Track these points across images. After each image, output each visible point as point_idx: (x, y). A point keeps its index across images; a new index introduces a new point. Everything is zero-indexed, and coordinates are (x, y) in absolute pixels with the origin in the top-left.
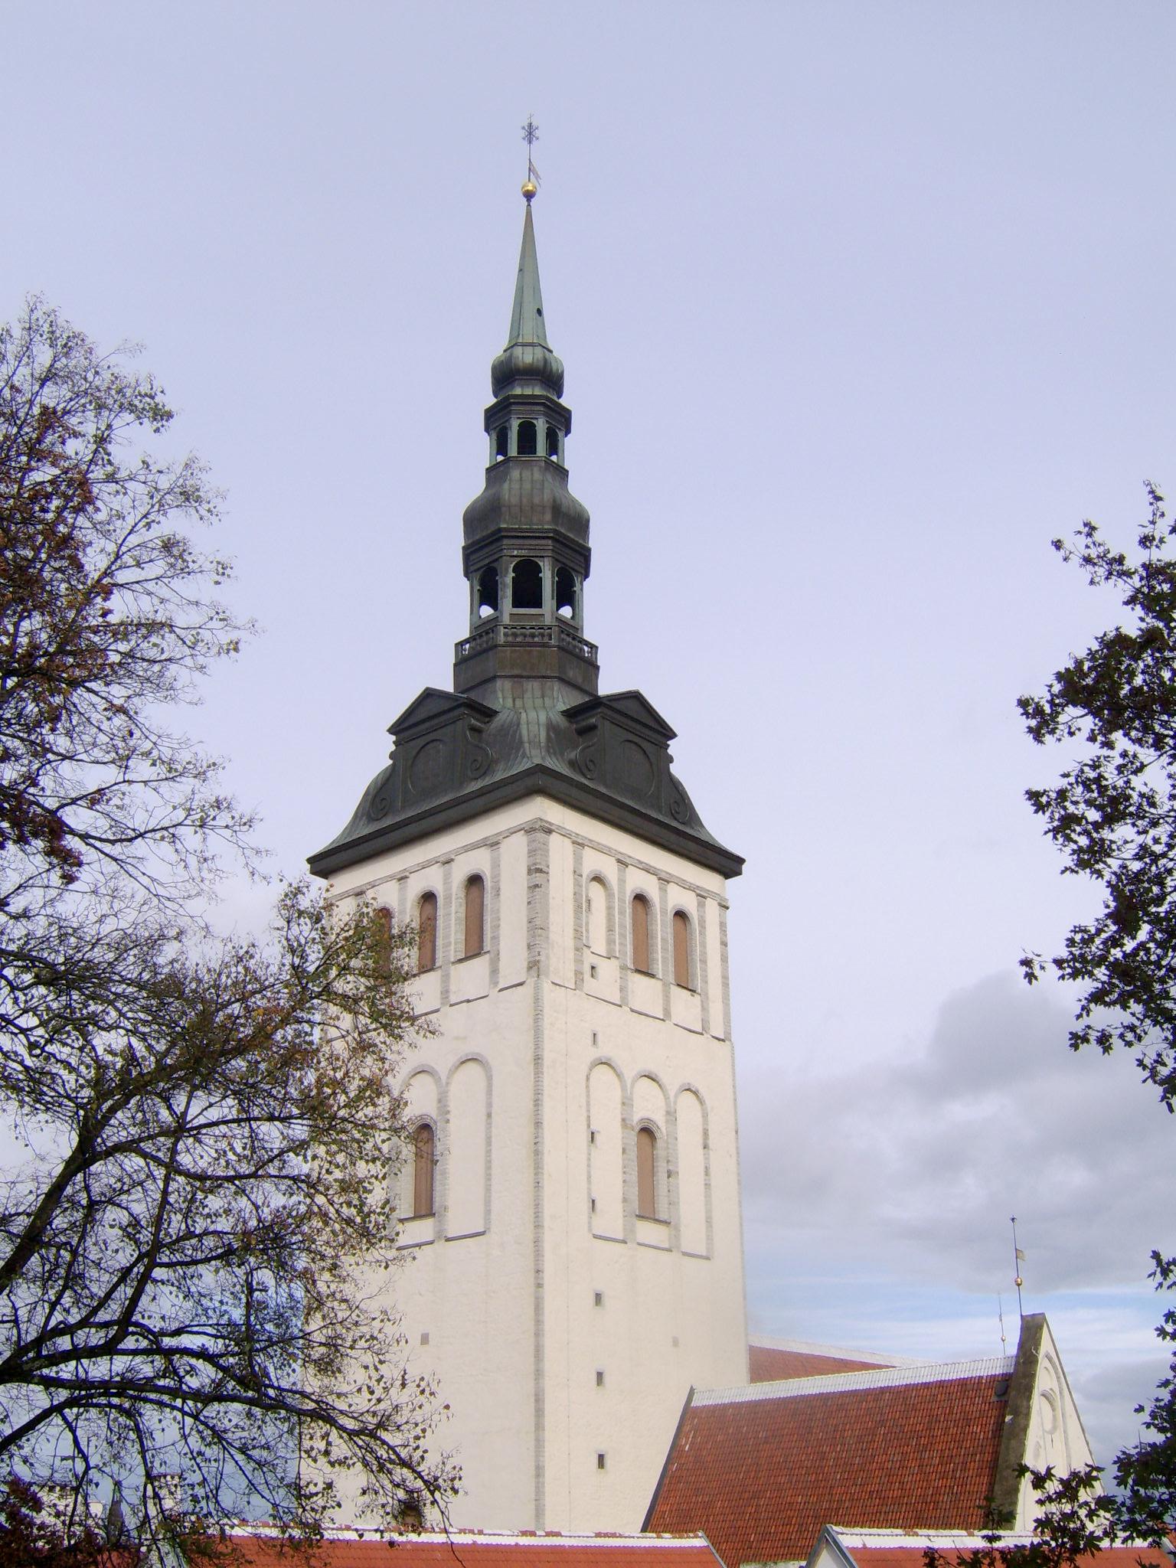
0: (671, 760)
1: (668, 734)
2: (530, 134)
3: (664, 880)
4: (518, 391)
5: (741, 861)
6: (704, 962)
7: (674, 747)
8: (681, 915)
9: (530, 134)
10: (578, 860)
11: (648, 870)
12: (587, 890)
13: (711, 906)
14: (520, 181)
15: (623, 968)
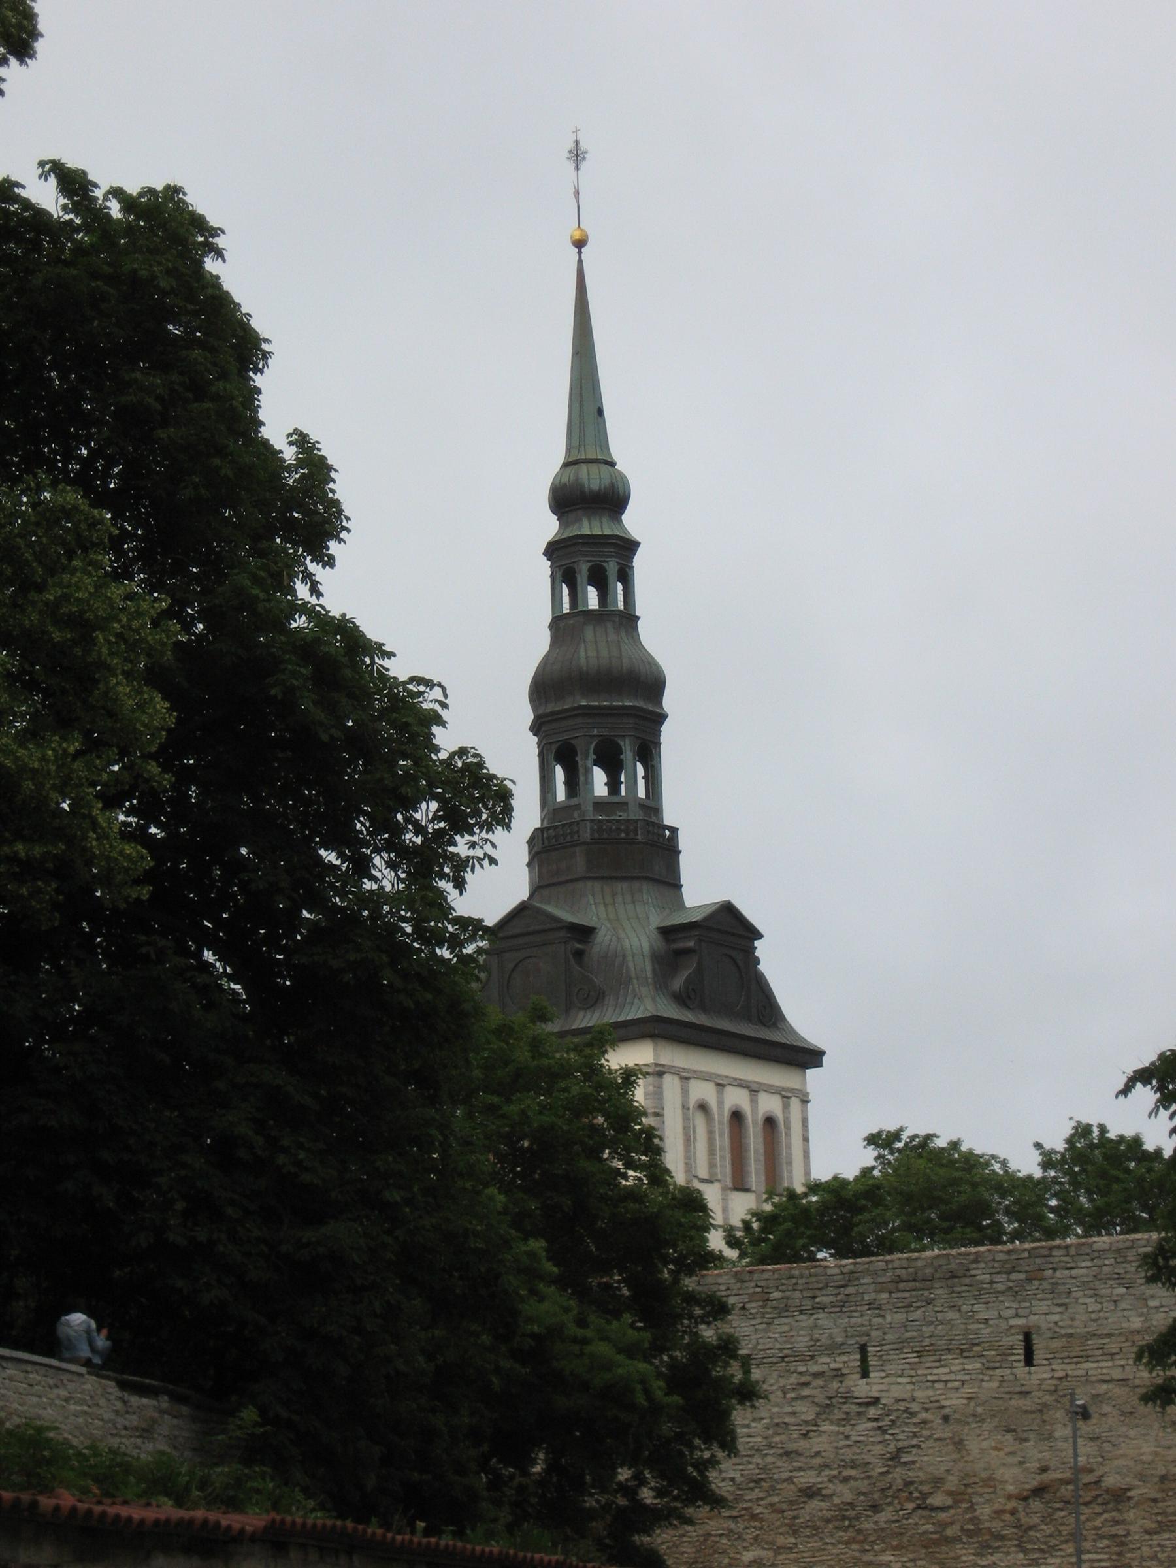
0: (757, 961)
1: (754, 934)
2: (577, 156)
3: (754, 1090)
4: (586, 531)
5: (822, 1053)
6: (790, 1163)
7: (761, 948)
8: (770, 1122)
9: (577, 156)
10: (685, 1092)
11: (741, 1084)
12: (693, 1120)
13: (795, 1103)
14: (570, 230)
15: (724, 1189)
